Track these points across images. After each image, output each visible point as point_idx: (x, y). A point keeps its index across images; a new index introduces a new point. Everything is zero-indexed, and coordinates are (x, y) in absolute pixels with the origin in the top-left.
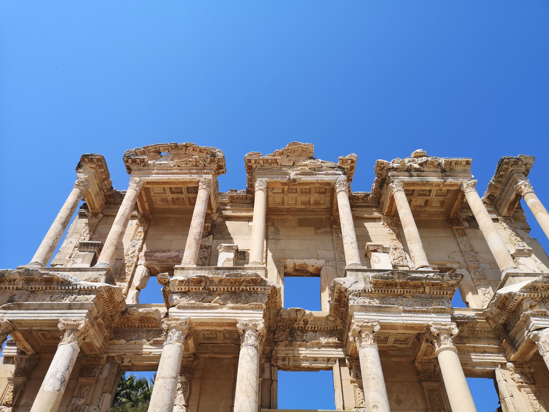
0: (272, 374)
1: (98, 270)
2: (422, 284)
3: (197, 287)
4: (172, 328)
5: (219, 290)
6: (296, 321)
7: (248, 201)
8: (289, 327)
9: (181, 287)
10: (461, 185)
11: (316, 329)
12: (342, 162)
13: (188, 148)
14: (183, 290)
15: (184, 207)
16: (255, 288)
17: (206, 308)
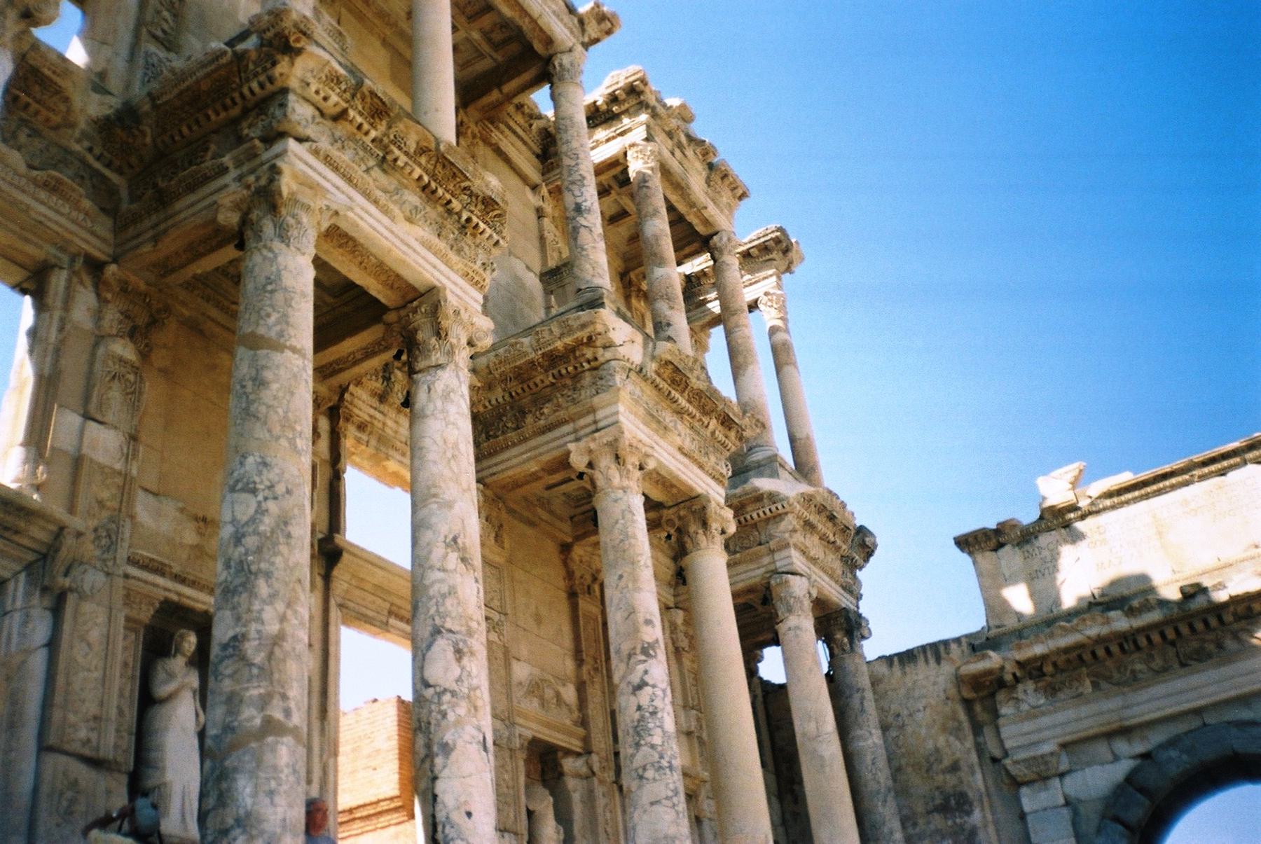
3: (366, 127)
5: (408, 170)
10: (716, 233)
14: (323, 105)
16: (482, 226)
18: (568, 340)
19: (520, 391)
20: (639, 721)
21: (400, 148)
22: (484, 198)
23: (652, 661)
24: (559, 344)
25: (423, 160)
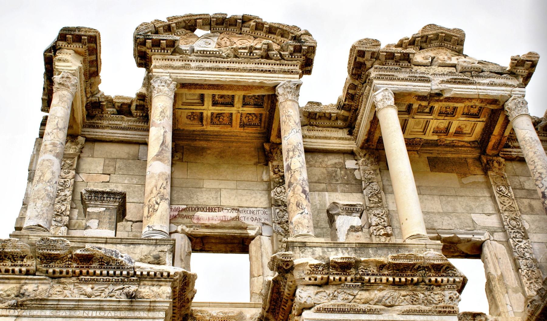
1: (157, 243)
7: (340, 123)
9: (315, 275)
13: (246, 25)
14: (316, 282)
15: (229, 129)
16: (439, 279)
21: (368, 275)
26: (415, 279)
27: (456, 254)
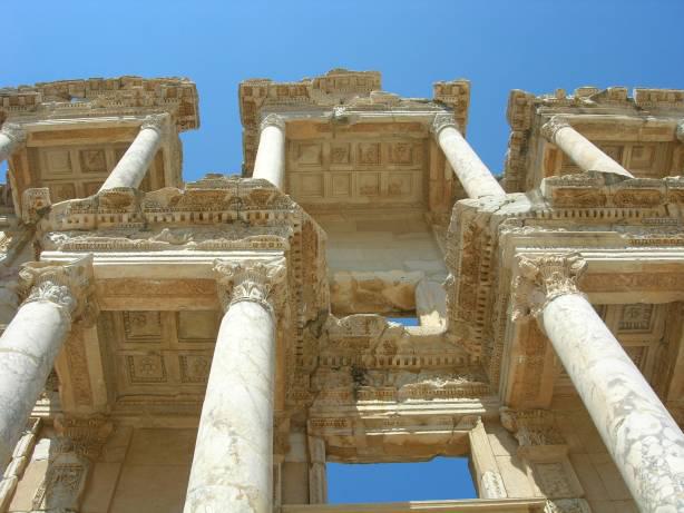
0: (311, 448)
2: (661, 197)
3: (116, 216)
4: (43, 280)
5: (169, 219)
6: (366, 347)
8: (349, 363)
11: (418, 362)
12: (442, 92)
14: (81, 224)
16: (263, 213)
17: (135, 248)
18: (462, 245)
19: (479, 315)
20: (641, 486)
21: (153, 211)
22: (252, 196)
23: (628, 417)
24: (463, 254)
25: (179, 206)
26: (225, 216)
27: (387, 309)
